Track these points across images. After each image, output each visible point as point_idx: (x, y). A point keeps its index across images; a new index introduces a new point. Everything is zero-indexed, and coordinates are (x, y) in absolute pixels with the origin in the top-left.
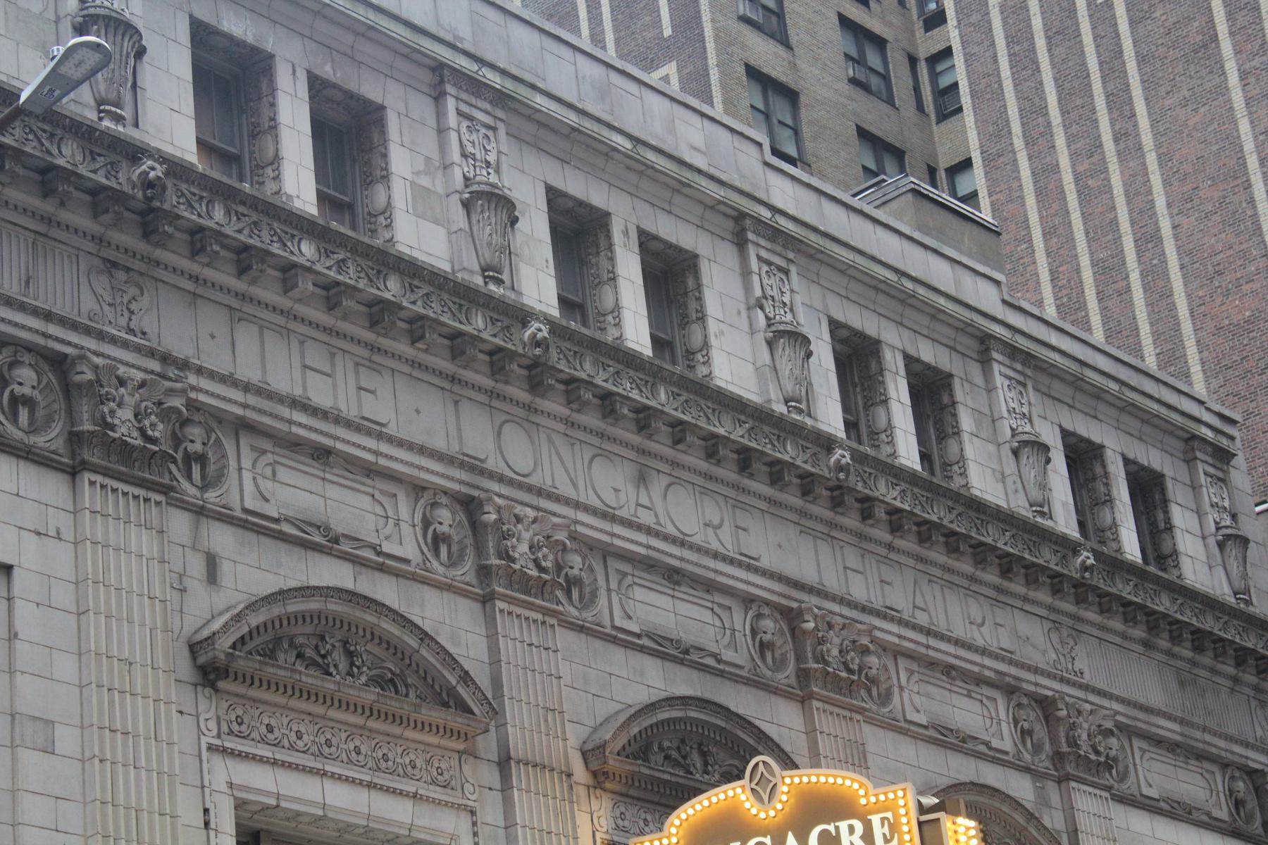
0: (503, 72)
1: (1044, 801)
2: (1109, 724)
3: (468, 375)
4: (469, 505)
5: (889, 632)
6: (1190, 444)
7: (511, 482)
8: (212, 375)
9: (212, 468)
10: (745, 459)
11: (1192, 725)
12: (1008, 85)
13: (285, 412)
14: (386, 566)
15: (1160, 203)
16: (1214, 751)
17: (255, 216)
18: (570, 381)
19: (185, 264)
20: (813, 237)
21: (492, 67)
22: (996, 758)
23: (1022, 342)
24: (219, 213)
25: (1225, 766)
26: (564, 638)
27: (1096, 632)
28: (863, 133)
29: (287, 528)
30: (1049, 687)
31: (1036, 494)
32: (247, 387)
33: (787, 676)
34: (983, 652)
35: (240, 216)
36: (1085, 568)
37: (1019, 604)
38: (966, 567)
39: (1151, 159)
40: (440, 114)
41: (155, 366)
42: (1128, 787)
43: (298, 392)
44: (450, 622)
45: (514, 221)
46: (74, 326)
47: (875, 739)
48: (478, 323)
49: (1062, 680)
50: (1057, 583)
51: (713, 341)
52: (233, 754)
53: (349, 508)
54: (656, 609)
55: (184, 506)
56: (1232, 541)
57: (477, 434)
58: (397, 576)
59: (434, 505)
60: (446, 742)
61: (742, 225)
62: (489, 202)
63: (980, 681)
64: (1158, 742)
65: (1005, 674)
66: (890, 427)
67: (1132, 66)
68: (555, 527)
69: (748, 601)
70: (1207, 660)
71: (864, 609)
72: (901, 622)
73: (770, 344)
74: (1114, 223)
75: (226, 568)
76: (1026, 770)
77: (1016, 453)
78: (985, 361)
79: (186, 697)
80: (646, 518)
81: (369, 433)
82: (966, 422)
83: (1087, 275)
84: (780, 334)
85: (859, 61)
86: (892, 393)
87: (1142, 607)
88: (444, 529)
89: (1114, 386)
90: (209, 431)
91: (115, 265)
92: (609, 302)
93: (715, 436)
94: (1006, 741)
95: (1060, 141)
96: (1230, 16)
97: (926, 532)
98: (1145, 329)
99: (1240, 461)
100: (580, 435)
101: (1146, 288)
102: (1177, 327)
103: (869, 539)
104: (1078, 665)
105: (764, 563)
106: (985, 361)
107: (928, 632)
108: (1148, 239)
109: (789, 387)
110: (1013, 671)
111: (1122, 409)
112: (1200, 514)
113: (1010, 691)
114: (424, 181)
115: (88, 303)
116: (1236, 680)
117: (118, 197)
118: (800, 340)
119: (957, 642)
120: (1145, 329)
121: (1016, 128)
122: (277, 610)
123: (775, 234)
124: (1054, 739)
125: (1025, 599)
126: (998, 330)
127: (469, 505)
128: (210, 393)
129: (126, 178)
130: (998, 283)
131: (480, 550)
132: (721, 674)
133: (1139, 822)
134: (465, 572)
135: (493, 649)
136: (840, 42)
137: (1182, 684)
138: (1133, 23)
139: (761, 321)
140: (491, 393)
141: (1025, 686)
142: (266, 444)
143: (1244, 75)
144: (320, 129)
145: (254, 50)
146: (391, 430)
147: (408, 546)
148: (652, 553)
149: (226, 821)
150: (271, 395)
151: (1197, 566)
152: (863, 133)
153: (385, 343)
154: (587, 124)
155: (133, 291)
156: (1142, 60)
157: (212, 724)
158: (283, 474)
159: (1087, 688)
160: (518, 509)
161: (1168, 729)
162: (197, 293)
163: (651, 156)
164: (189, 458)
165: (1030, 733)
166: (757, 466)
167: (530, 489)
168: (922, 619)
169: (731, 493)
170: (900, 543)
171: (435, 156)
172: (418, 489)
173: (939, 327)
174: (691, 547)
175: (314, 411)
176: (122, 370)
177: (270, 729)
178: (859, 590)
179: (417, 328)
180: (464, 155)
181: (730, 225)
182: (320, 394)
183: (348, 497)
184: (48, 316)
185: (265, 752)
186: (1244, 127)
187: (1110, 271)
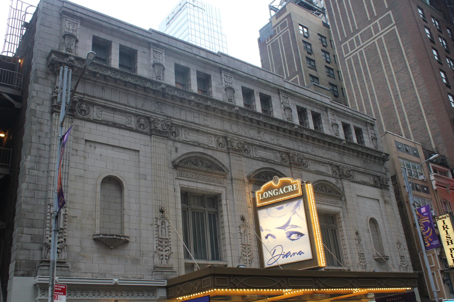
0: (232, 68)
1: (337, 182)
2: (350, 169)
3: (225, 117)
4: (226, 138)
5: (307, 156)
6: (366, 123)
7: (233, 134)
8: (176, 119)
9: (177, 134)
10: (278, 128)
11: (366, 169)
12: (349, 72)
13: (190, 124)
14: (209, 148)
15: (374, 89)
17: (183, 93)
18: (244, 117)
19: (171, 101)
20: (292, 92)
21: (230, 67)
22: (328, 176)
23: (333, 108)
24: (176, 93)
25: (373, 175)
26: (244, 159)
28: (330, 84)
30: (338, 164)
31: (336, 132)
32: (183, 120)
33: (287, 164)
34: (326, 158)
35: (180, 93)
36: (344, 144)
38: (322, 145)
39: (372, 82)
40: (221, 76)
41: (166, 118)
42: (354, 179)
43: (192, 121)
44: (222, 158)
45: (234, 92)
46: (151, 112)
47: (304, 173)
48: (225, 108)
49: (341, 162)
50: (339, 146)
51: (274, 110)
52: (180, 179)
53: (203, 139)
54: (262, 153)
55: (171, 140)
56: (374, 139)
57: (227, 126)
59: (219, 138)
60: (221, 176)
61: (279, 91)
62: (229, 89)
63: (325, 163)
64: (360, 172)
66: (308, 123)
67: (368, 68)
68: (241, 141)
69: (280, 152)
70: (369, 158)
71: (302, 152)
72: (309, 154)
73: (284, 110)
74: (367, 93)
75: (179, 150)
76: (334, 177)
77: (332, 126)
78: (326, 111)
79: (171, 170)
80: (259, 139)
81: (206, 127)
82: (323, 121)
83: (363, 101)
84: (286, 108)
85: (329, 72)
86: (309, 117)
87: (356, 150)
88: (221, 142)
89: (351, 114)
90: (176, 128)
92: (254, 104)
93: (272, 125)
94: (330, 173)
95: (357, 81)
96: (383, 58)
97: (314, 139)
98: (372, 109)
99: (376, 125)
100: (247, 126)
101: (372, 103)
102: (377, 108)
103: (297, 139)
104: (344, 160)
105: (283, 145)
106: (326, 111)
107: (315, 156)
108: (372, 95)
109: (288, 116)
110: (331, 161)
112: (368, 135)
113: (331, 165)
114: (218, 86)
115: (154, 108)
116: (375, 161)
117: (157, 91)
118: (289, 109)
119: (320, 157)
120: (372, 109)
121: (351, 79)
122: (187, 156)
123: (285, 92)
124: (339, 172)
126: (328, 106)
127: (226, 138)
128: (176, 122)
129: (159, 88)
131: (227, 145)
132: (275, 164)
133: (356, 185)
134: (225, 149)
135: (230, 161)
136: (325, 70)
137: (364, 162)
138: (367, 61)
139: (282, 106)
140: (229, 120)
142: (187, 130)
143: (385, 67)
144: (199, 79)
145: (187, 68)
146: (210, 126)
147: (214, 145)
149: (179, 190)
150: (187, 121)
151: (368, 143)
152: (330, 84)
153: (209, 112)
154: (248, 76)
155: (162, 106)
156: (369, 66)
157: (176, 175)
158: (190, 134)
159: (346, 164)
160: (234, 138)
161: (362, 170)
162: (174, 106)
163: (261, 80)
164: (172, 132)
165: (335, 171)
166: (280, 129)
167: (237, 135)
168: (314, 153)
169: (276, 134)
170: (309, 141)
171: (220, 82)
172: (216, 136)
174: (268, 143)
175: (195, 124)
176: (159, 119)
177: (187, 175)
178: (301, 149)
179: (214, 109)
180: (225, 82)
181: (277, 91)
182: (197, 121)
183: (202, 137)
184: (146, 111)
185: (186, 179)
186: (386, 75)
187: (366, 100)
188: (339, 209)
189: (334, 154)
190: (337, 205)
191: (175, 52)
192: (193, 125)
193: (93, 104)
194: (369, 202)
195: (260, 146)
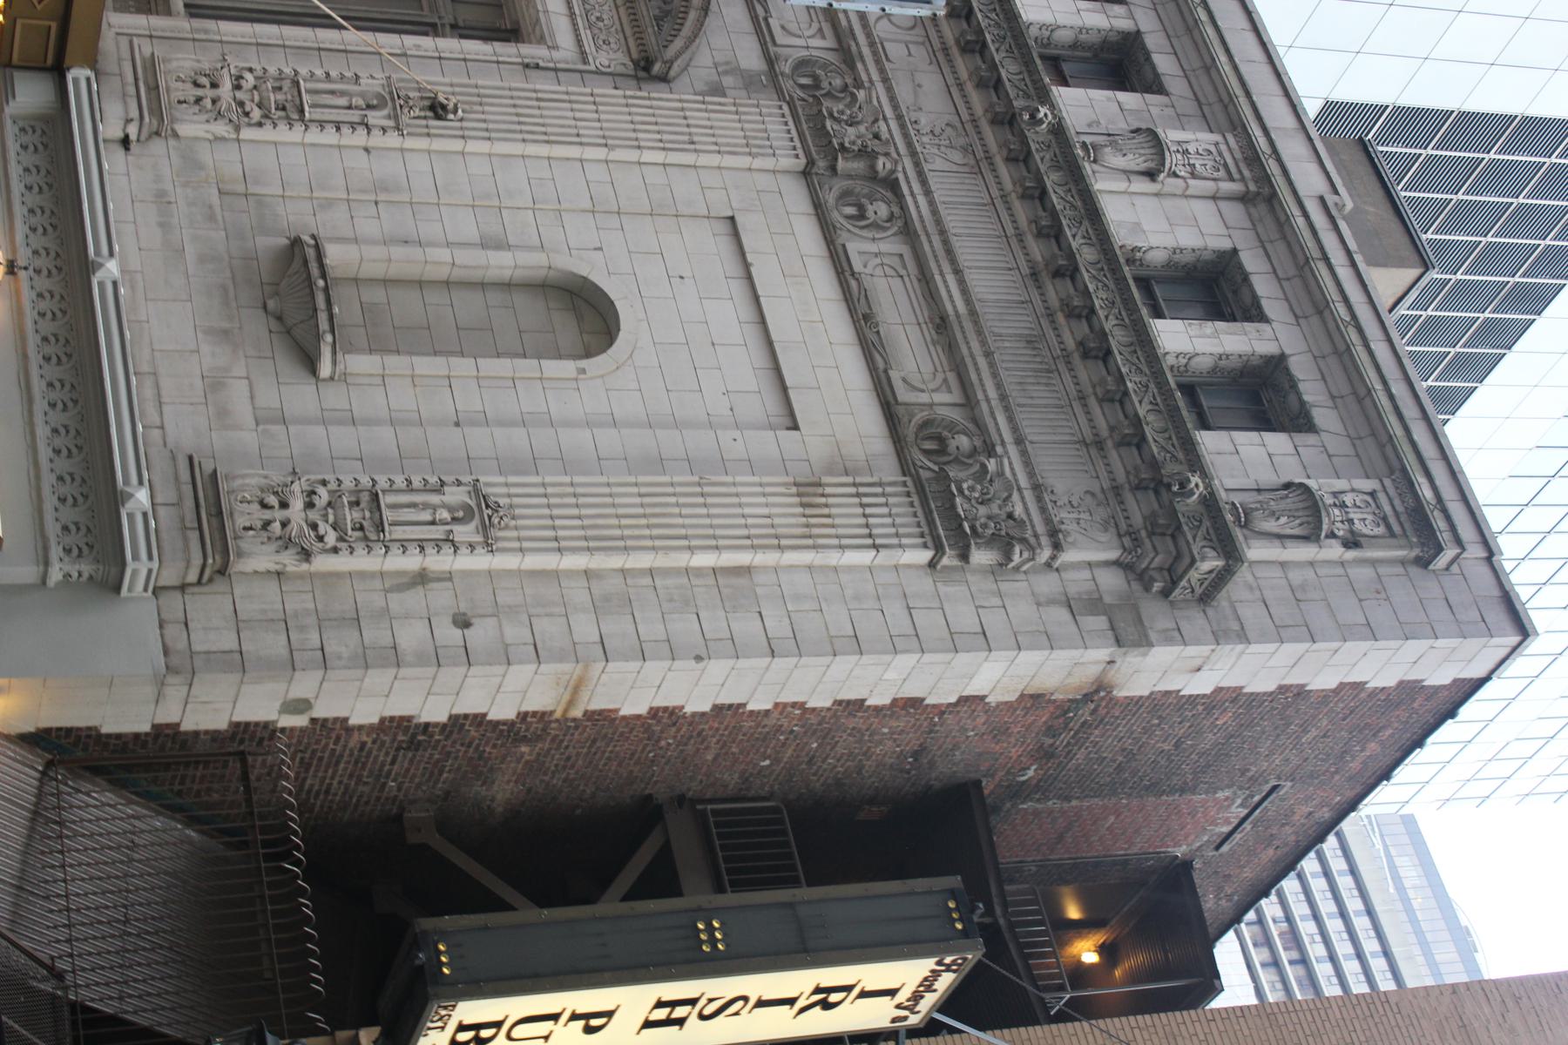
16: (974, 376)
25: (969, 402)
27: (995, 193)
37: (951, 81)
65: (855, 39)
70: (1087, 373)
76: (770, 61)
110: (866, 51)
111: (1336, 352)
125: (960, 86)
126: (1256, 131)
130: (1336, 192)
141: (859, 66)
161: (954, 302)
173: (1204, 80)
188: (564, 38)
189: (931, 82)
190: (586, 36)
194: (729, 315)
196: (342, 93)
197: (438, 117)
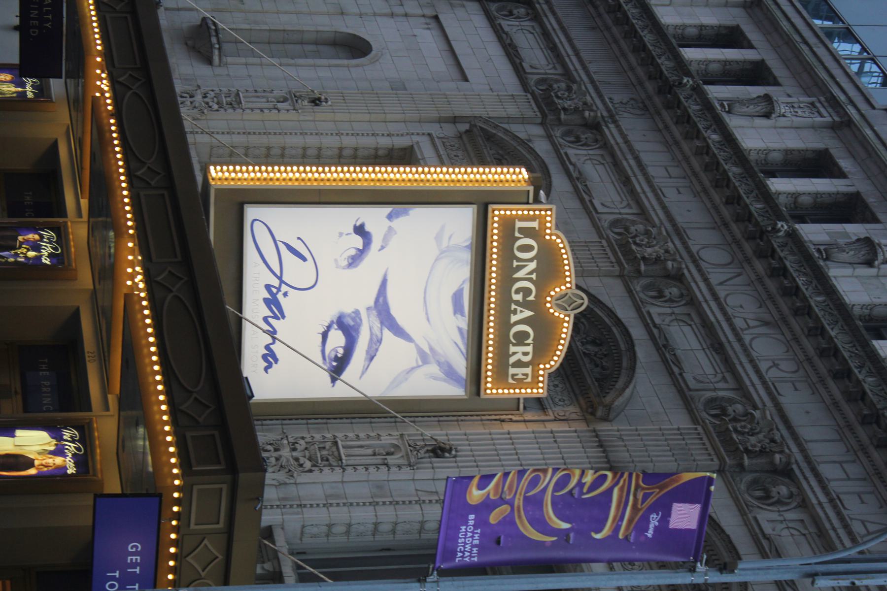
29: (571, 168)
58: (585, 208)
91: (643, 103)
129: (673, 78)
148: (716, 324)
158: (600, 168)
169: (815, 379)
191: (864, 142)
192: (632, 162)
193: (536, 17)
195: (708, 330)
196: (368, 447)
197: (317, 105)
